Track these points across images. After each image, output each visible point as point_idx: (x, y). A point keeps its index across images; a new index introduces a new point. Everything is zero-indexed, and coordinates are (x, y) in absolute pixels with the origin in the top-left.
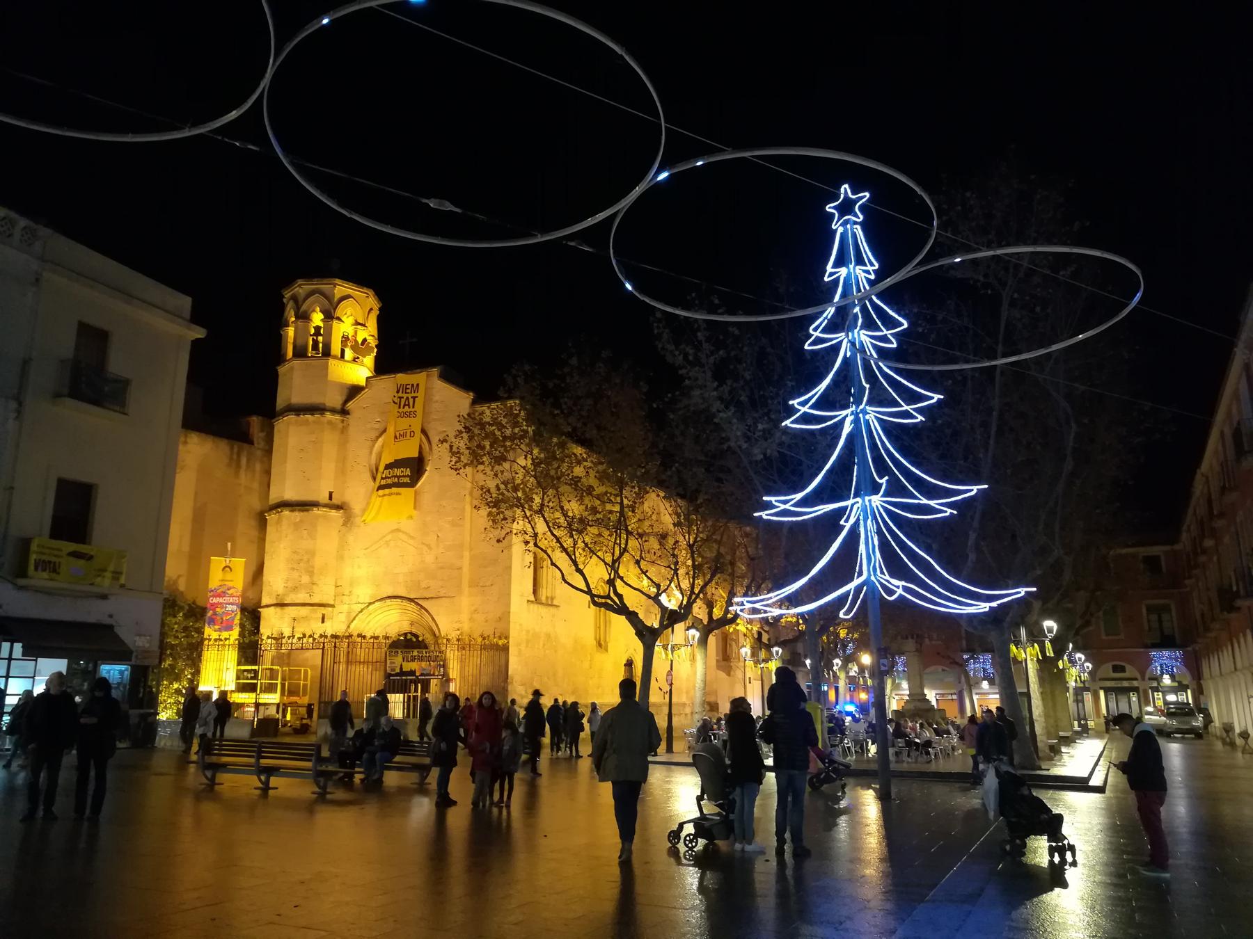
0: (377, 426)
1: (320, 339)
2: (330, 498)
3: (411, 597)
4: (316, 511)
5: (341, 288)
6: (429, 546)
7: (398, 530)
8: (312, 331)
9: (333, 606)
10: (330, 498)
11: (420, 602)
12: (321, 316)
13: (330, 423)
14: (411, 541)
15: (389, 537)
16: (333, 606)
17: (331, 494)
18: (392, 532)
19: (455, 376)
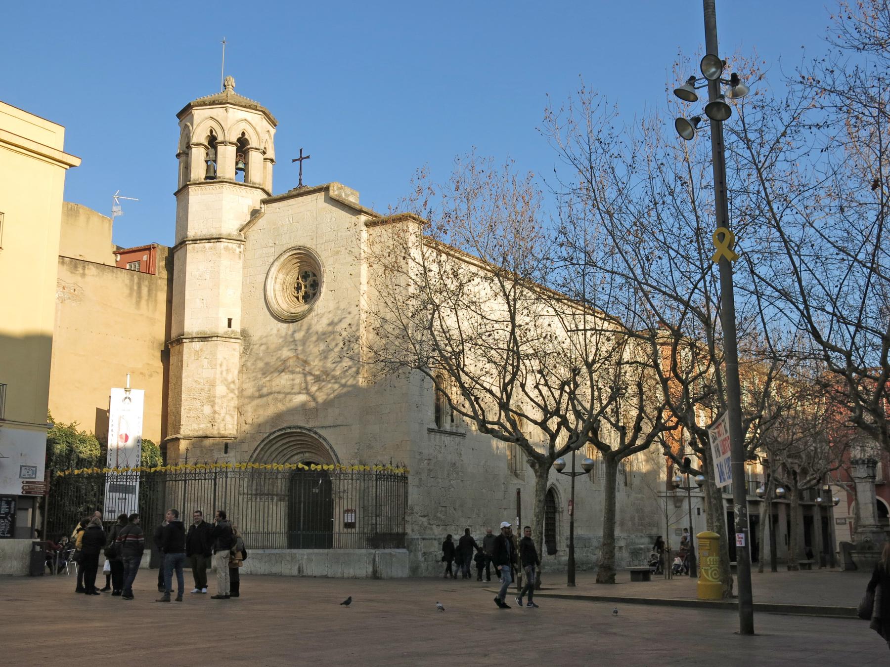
2: (230, 326)
10: (230, 326)
11: (319, 431)
17: (230, 320)
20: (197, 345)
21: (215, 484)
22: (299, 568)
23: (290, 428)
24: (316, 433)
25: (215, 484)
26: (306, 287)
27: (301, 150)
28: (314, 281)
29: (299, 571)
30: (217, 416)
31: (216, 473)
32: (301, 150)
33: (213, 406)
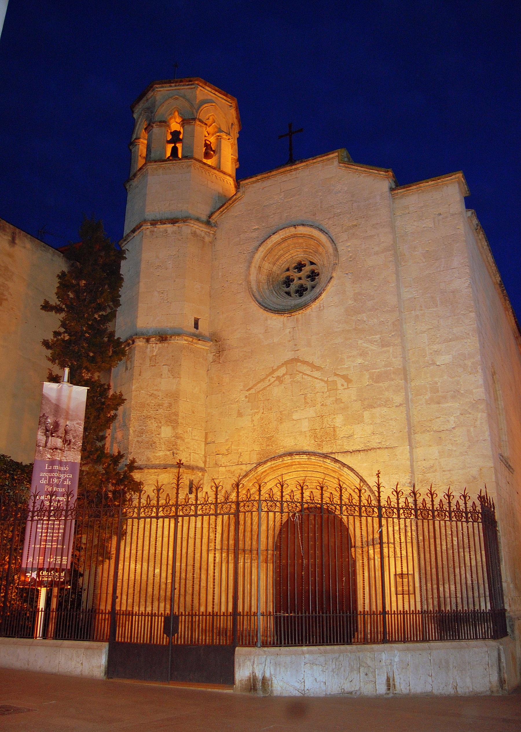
0: (255, 235)
1: (179, 146)
2: (196, 326)
3: (326, 450)
4: (182, 341)
5: (204, 92)
6: (345, 378)
7: (296, 360)
8: (169, 137)
9: (202, 470)
10: (196, 326)
11: (339, 457)
12: (179, 120)
13: (194, 234)
14: (317, 374)
15: (283, 370)
16: (202, 470)
18: (286, 363)
19: (363, 154)
20: (155, 348)
21: (237, 523)
22: (388, 680)
23: (291, 454)
24: (336, 461)
25: (237, 523)
26: (300, 278)
27: (290, 126)
28: (313, 272)
29: (388, 685)
30: (179, 441)
31: (238, 504)
32: (290, 126)
33: (174, 428)
